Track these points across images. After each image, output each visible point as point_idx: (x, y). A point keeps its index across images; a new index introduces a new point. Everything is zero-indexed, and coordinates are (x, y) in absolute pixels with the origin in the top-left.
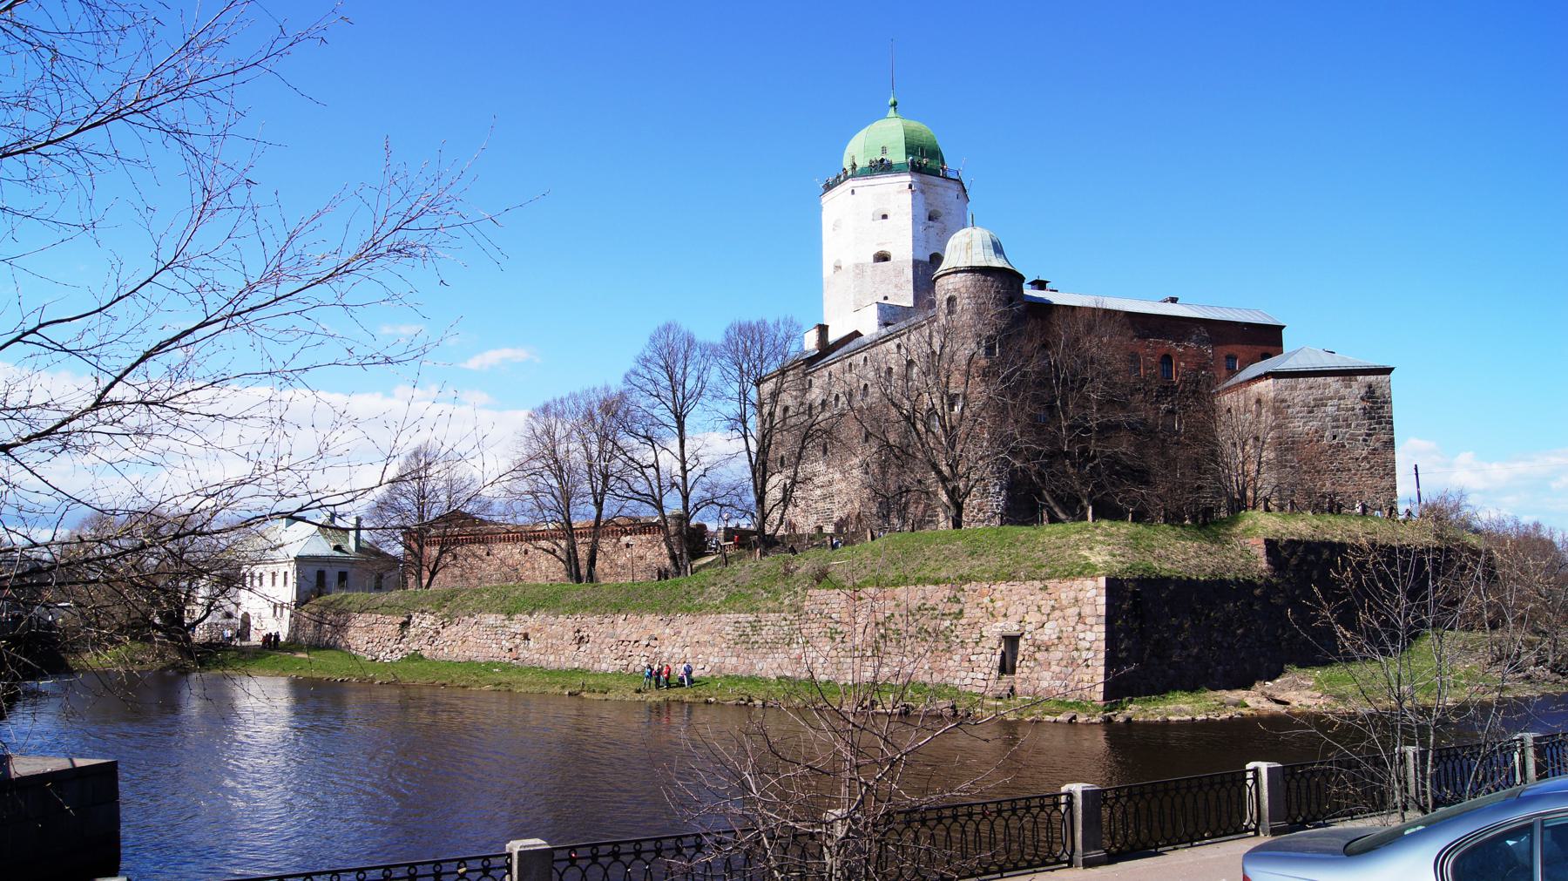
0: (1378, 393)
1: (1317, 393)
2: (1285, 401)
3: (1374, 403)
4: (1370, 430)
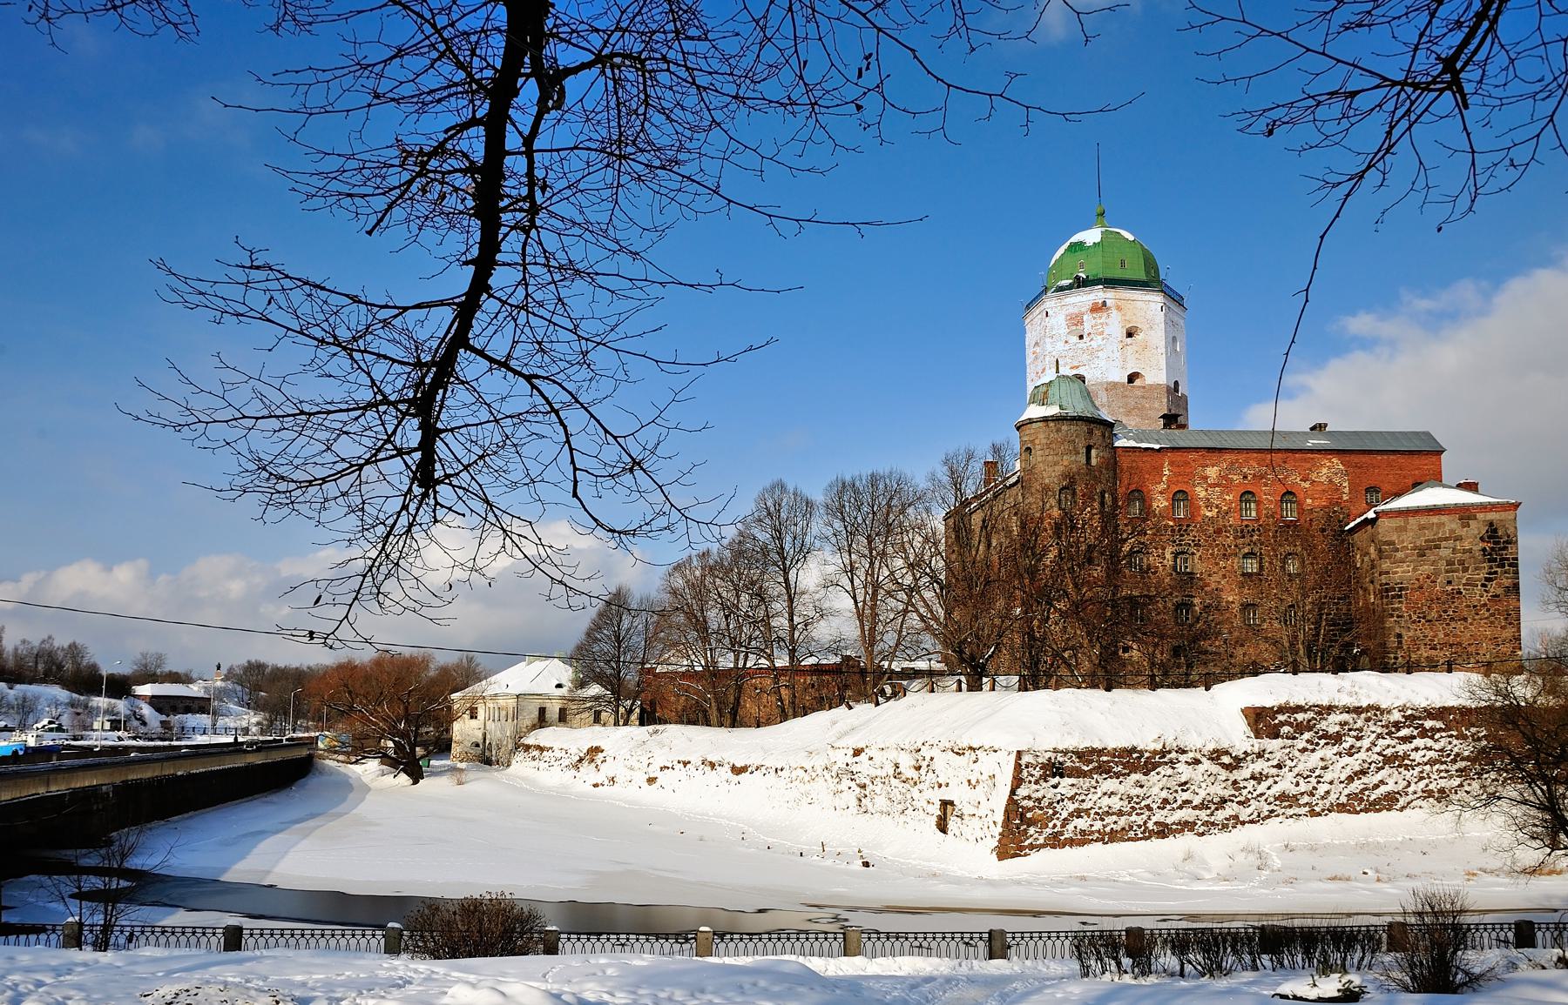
1: (1429, 535)
2: (1391, 543)
3: (1495, 543)
4: (1490, 573)
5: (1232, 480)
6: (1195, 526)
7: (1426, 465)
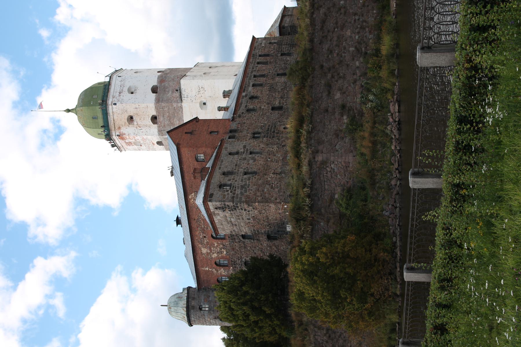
0: (219, 206)
5: (207, 242)
6: (232, 258)
7: (186, 155)
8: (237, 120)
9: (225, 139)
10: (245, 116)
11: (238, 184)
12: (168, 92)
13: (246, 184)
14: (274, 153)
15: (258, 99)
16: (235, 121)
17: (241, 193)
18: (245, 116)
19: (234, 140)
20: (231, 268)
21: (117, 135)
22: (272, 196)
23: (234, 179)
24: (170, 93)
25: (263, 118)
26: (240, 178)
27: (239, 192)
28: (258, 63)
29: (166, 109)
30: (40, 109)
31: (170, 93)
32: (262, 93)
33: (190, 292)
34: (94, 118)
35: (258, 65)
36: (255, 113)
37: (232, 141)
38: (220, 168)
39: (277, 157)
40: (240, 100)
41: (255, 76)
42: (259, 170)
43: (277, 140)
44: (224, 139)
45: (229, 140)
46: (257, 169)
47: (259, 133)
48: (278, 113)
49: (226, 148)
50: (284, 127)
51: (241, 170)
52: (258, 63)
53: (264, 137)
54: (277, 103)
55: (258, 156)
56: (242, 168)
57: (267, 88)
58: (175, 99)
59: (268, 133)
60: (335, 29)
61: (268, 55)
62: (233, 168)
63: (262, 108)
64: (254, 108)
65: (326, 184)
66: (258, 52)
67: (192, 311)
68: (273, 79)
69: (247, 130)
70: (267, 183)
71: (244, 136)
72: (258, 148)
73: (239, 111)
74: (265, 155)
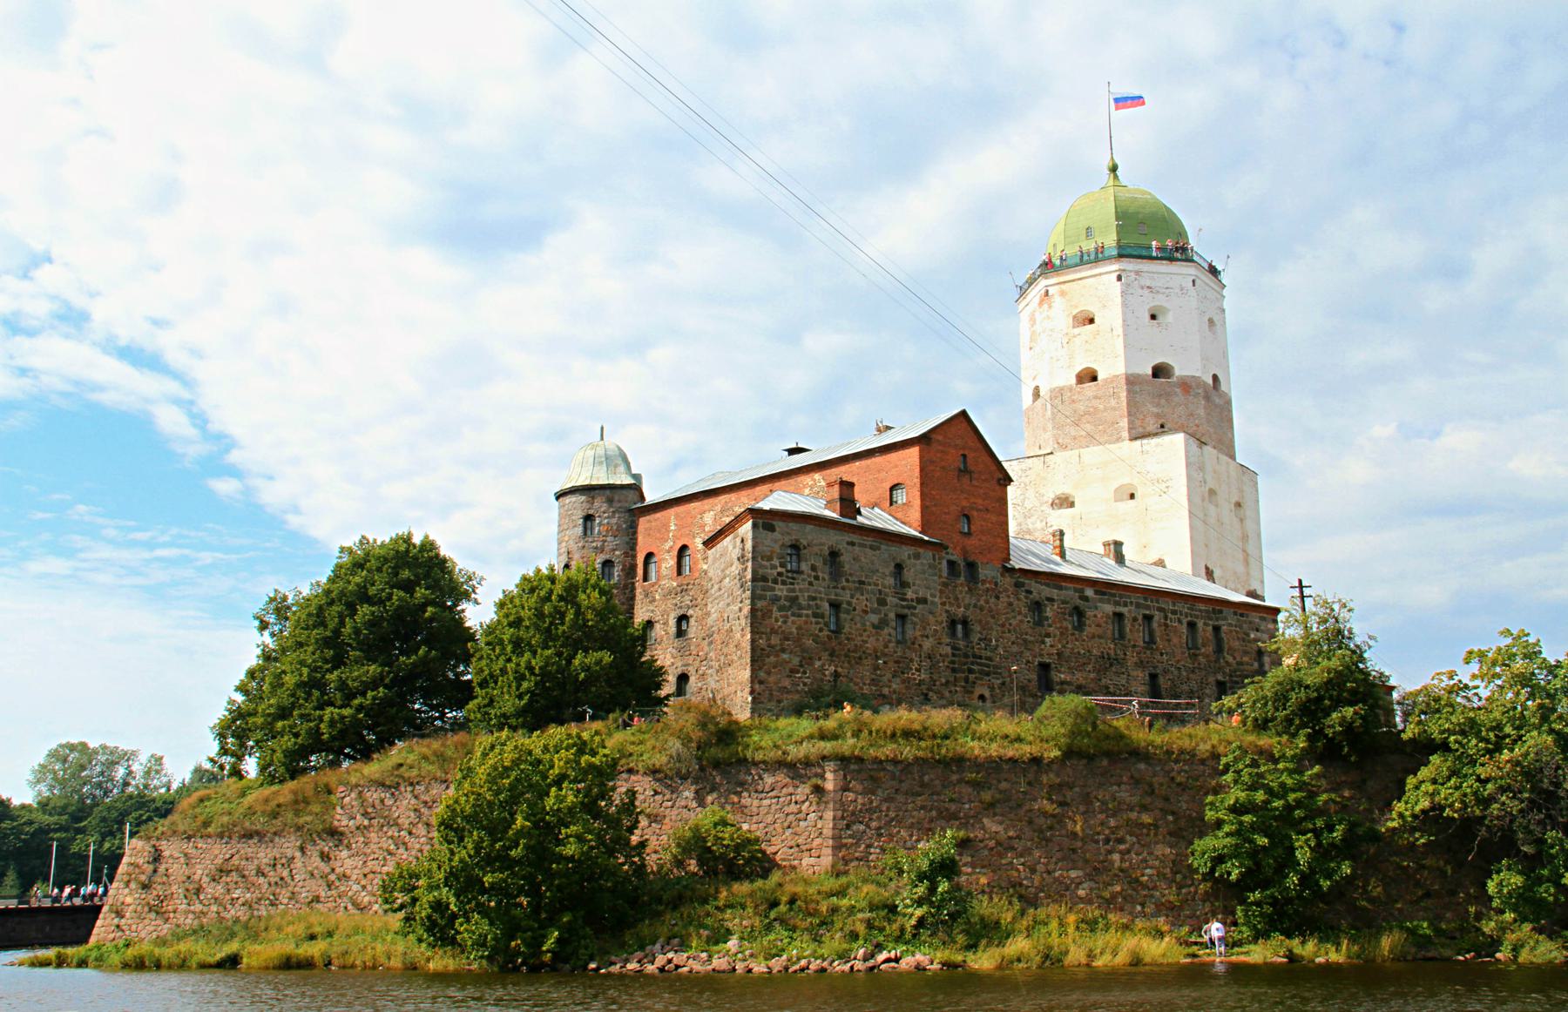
8: (1008, 579)
9: (947, 553)
10: (1019, 599)
11: (801, 590)
12: (1158, 405)
13: (801, 608)
14: (903, 673)
15: (1075, 628)
16: (1002, 575)
17: (776, 599)
18: (1019, 599)
19: (945, 574)
20: (675, 584)
21: (1047, 291)
22: (769, 673)
23: (817, 578)
24: (1155, 410)
25: (1013, 643)
26: (820, 593)
27: (779, 593)
28: (1192, 626)
29: (1113, 403)
30: (1117, 100)
31: (1155, 410)
32: (1093, 637)
33: (624, 492)
34: (1089, 232)
35: (1185, 625)
36: (1028, 622)
37: (940, 570)
38: (852, 544)
39: (890, 681)
40: (1071, 582)
41: (1148, 618)
42: (848, 639)
43: (943, 681)
44: (946, 548)
45: (945, 563)
46: (850, 633)
47: (967, 633)
48: (1029, 681)
49: (917, 556)
50: (987, 694)
51: (845, 596)
52: (1192, 626)
53: (954, 648)
54: (1062, 676)
55: (890, 635)
56: (852, 597)
57: (1110, 648)
58: (1138, 423)
59: (966, 656)
60: (1173, 813)
61: (1219, 649)
62: (851, 575)
63: (1047, 640)
64: (1047, 619)
65: (774, 801)
66: (1230, 625)
67: (583, 498)
68: (1141, 664)
69: (975, 606)
70: (804, 658)
71: (957, 599)
72: (918, 633)
73: (1036, 582)
74: (896, 652)
